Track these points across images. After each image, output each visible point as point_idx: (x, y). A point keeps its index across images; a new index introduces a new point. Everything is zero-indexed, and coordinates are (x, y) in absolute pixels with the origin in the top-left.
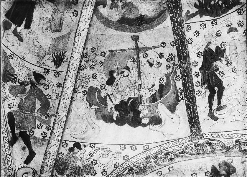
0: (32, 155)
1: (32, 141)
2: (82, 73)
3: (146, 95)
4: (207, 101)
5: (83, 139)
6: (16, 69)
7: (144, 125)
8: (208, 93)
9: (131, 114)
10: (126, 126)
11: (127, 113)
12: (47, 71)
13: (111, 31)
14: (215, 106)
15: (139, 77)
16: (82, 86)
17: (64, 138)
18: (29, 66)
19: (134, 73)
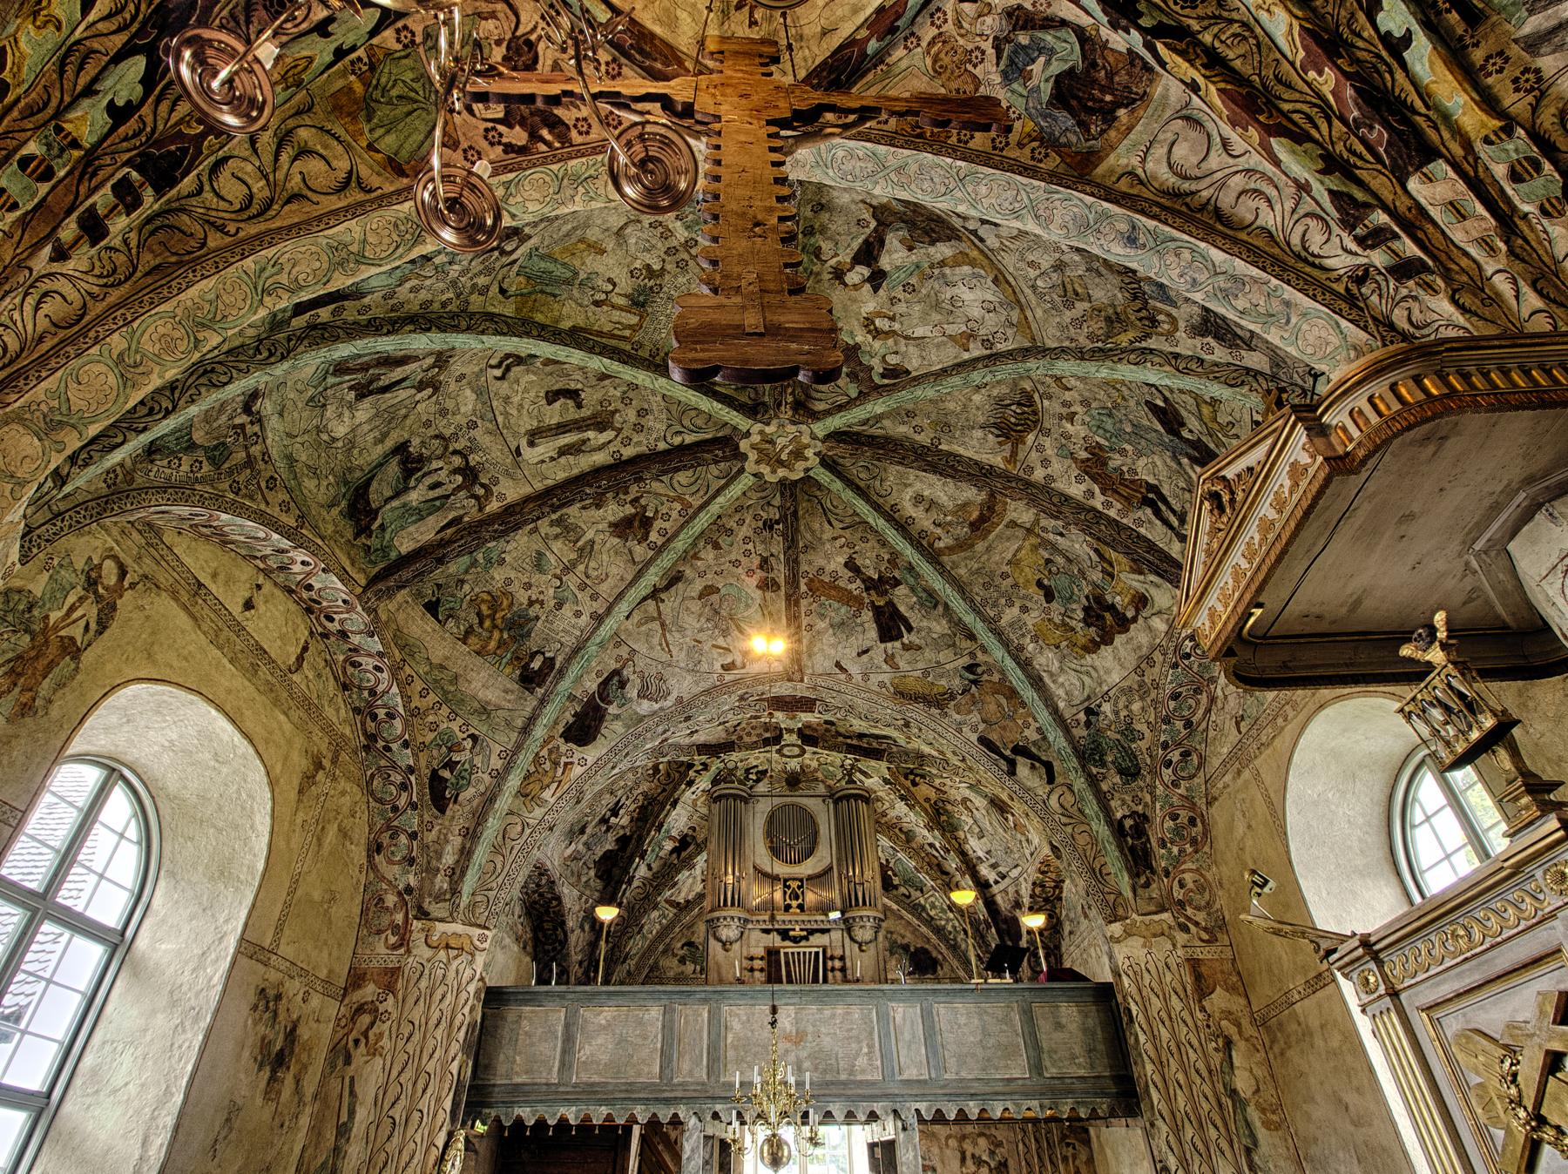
0: (1049, 767)
1: (1034, 750)
2: (1003, 622)
3: (1096, 576)
4: (1158, 522)
5: (1089, 698)
6: (943, 682)
7: (1134, 619)
8: (1149, 511)
9: (1108, 615)
10: (1119, 639)
11: (1103, 618)
12: (972, 654)
13: (980, 546)
14: (1175, 522)
15: (1069, 561)
16: (1023, 635)
17: (1067, 715)
18: (952, 666)
19: (1060, 560)
